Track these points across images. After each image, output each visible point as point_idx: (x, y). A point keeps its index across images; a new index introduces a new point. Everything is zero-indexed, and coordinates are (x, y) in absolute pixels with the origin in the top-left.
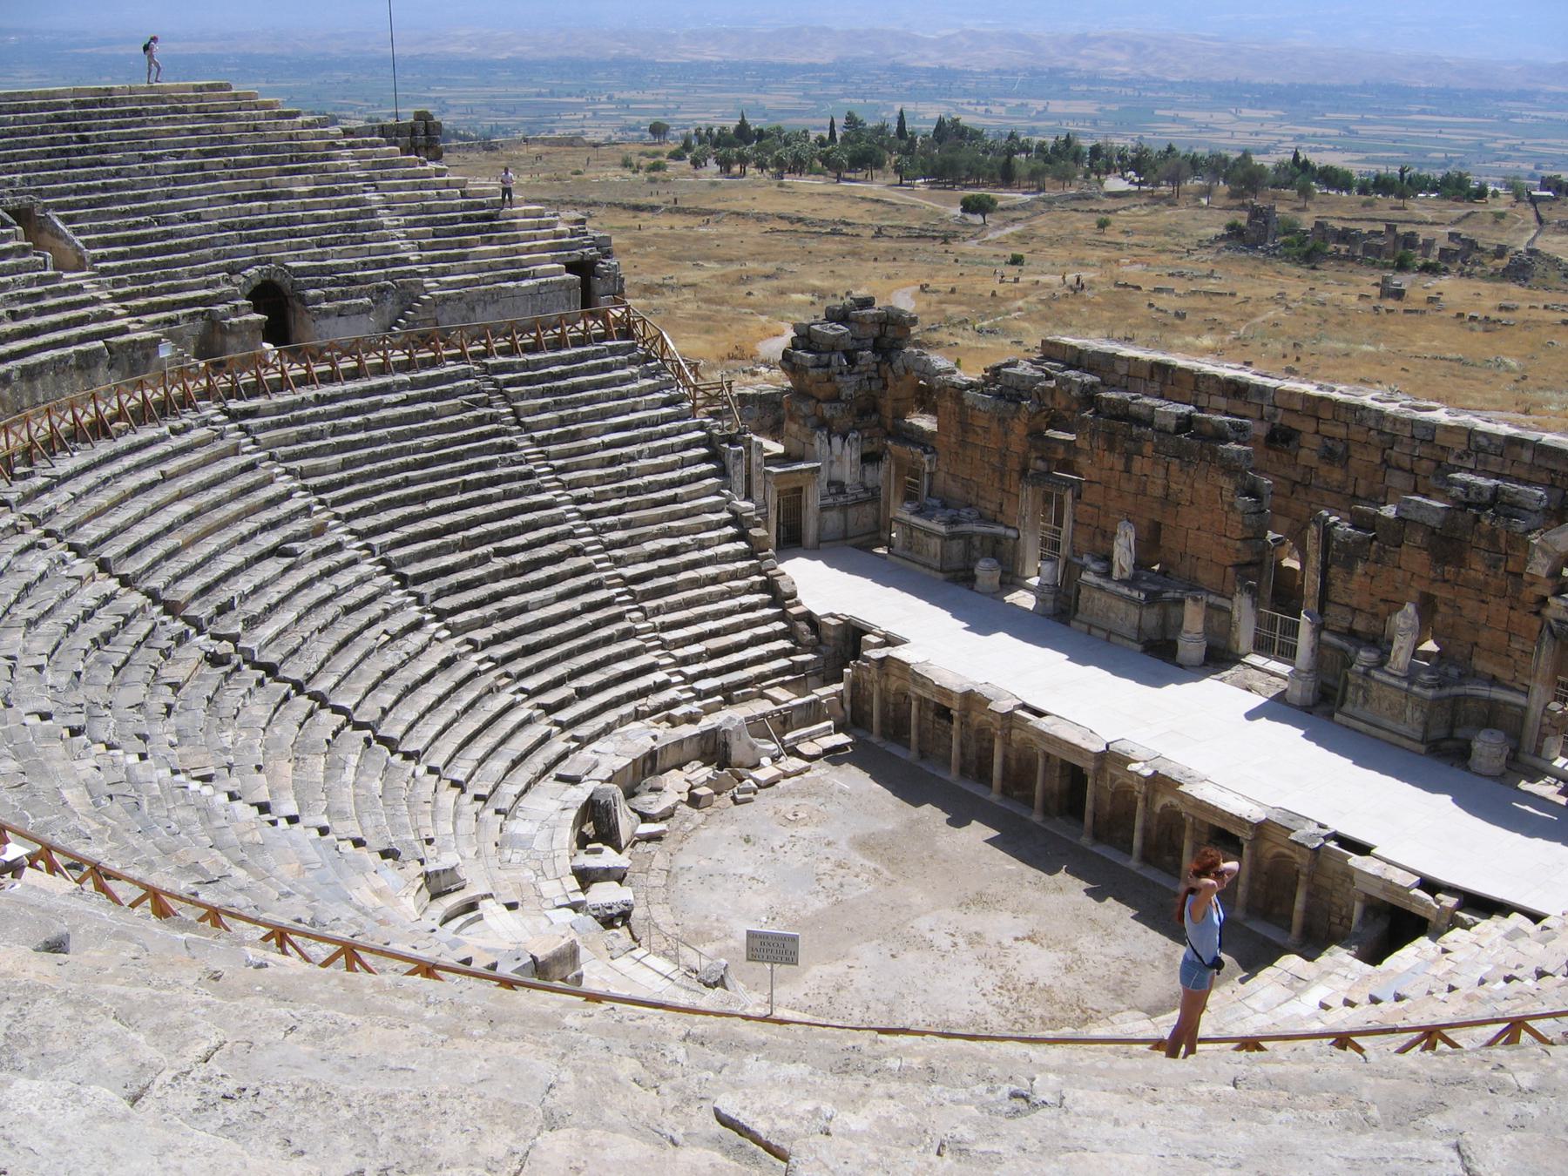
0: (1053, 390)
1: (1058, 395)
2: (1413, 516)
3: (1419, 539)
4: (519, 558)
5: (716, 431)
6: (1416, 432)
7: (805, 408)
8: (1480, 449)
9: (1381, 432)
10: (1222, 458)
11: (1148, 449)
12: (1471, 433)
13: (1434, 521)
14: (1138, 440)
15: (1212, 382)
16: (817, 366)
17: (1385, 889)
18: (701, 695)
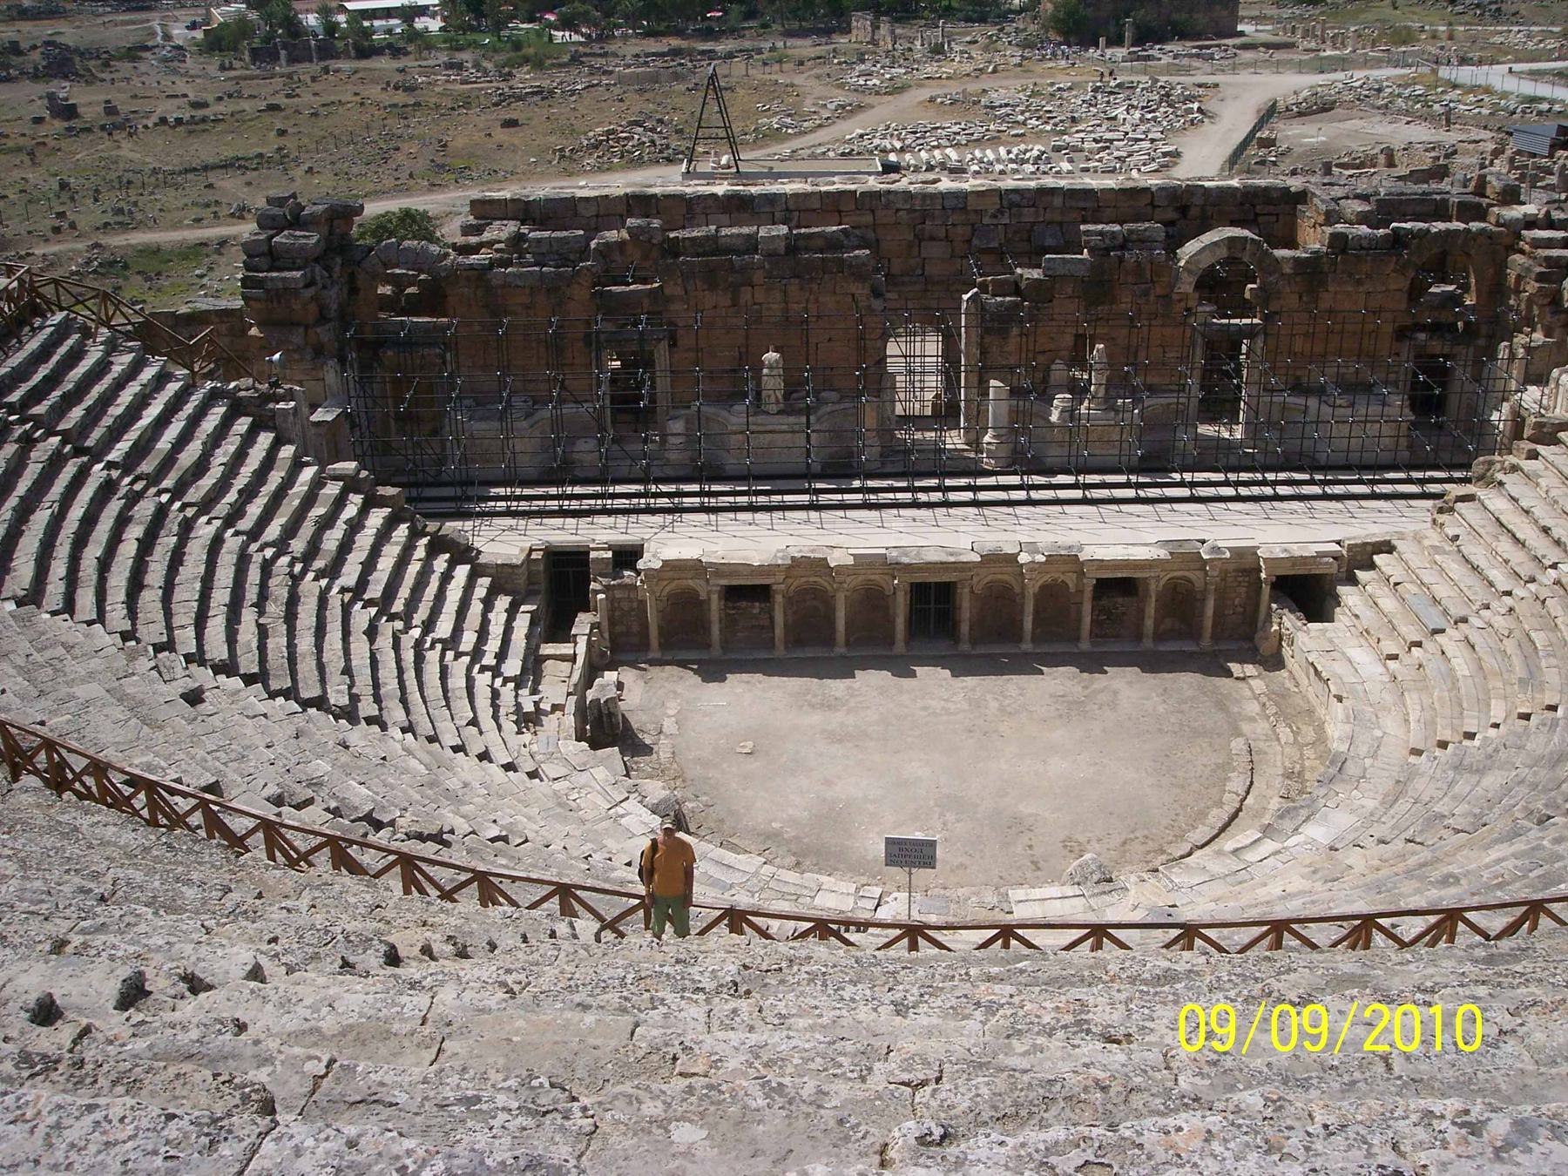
0: (621, 244)
1: (630, 249)
2: (1060, 271)
3: (1070, 291)
4: (275, 609)
5: (242, 394)
6: (948, 204)
7: (297, 337)
8: (1012, 205)
9: (910, 211)
10: (850, 266)
11: (758, 277)
12: (999, 193)
13: (1082, 271)
14: (743, 269)
15: (710, 202)
16: (307, 286)
17: (1294, 565)
18: (519, 682)
